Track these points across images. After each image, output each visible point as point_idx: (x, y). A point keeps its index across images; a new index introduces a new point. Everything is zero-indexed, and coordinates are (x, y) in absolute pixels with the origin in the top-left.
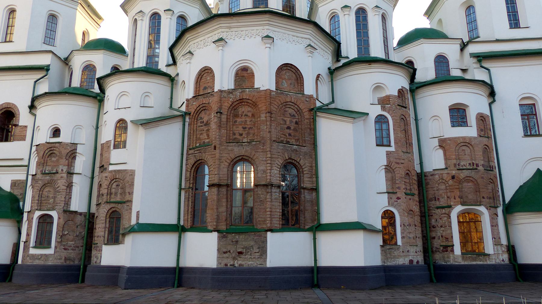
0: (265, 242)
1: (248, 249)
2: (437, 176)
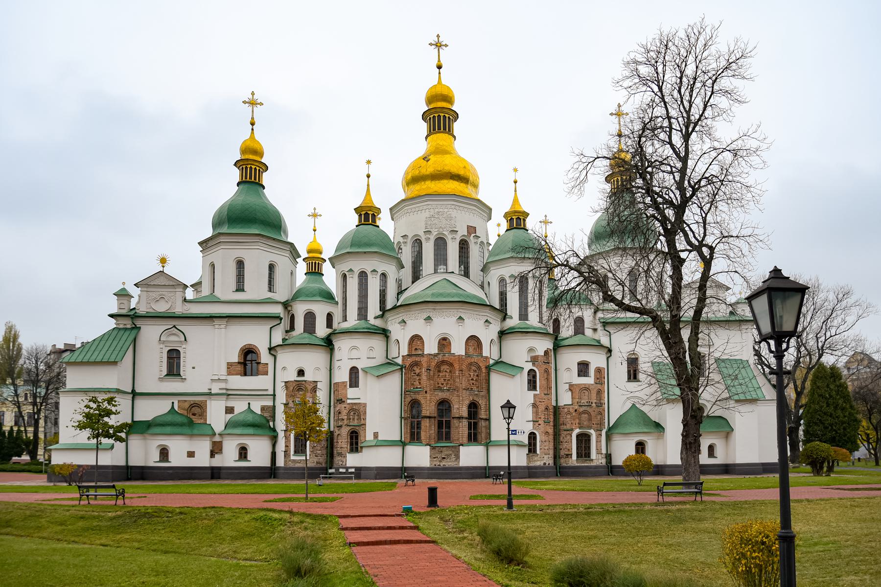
0: (459, 451)
1: (449, 456)
2: (566, 409)
